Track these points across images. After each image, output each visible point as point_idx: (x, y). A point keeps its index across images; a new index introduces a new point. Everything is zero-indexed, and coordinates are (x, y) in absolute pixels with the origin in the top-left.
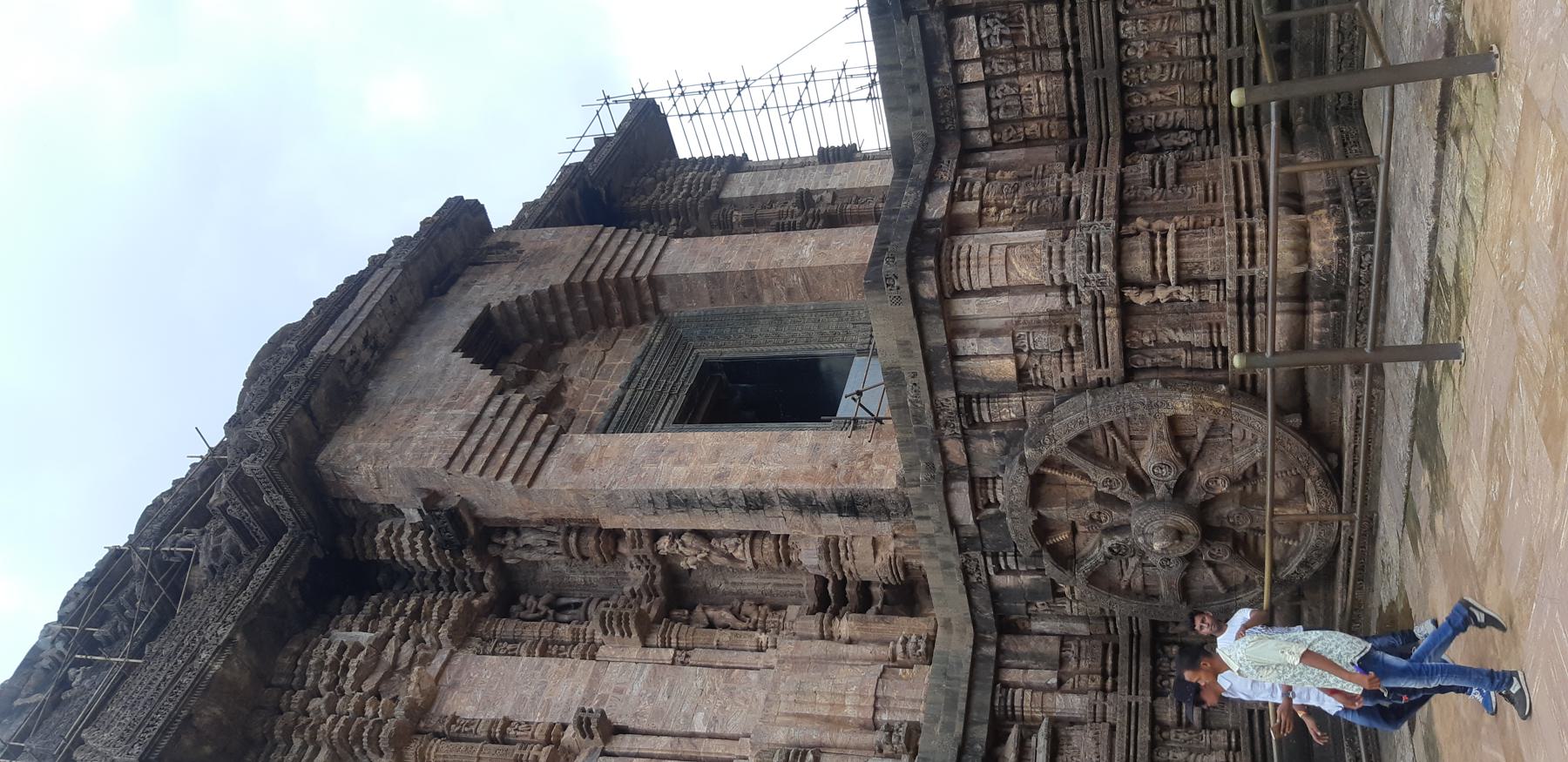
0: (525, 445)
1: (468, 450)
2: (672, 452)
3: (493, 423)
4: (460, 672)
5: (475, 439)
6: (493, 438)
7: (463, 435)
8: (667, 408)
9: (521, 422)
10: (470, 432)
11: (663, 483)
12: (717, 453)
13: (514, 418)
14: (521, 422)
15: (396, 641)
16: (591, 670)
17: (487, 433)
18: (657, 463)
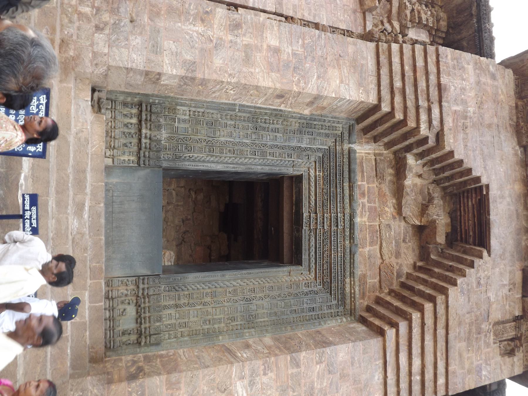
0: (398, 84)
1: (432, 68)
2: (287, 66)
3: (428, 100)
4: (356, 21)
5: (433, 78)
6: (422, 84)
7: (442, 79)
8: (313, 194)
9: (410, 104)
10: (439, 85)
11: (282, 28)
12: (247, 60)
13: (417, 108)
14: (410, 104)
15: (396, 31)
16: (284, 8)
17: (428, 86)
18: (294, 54)
